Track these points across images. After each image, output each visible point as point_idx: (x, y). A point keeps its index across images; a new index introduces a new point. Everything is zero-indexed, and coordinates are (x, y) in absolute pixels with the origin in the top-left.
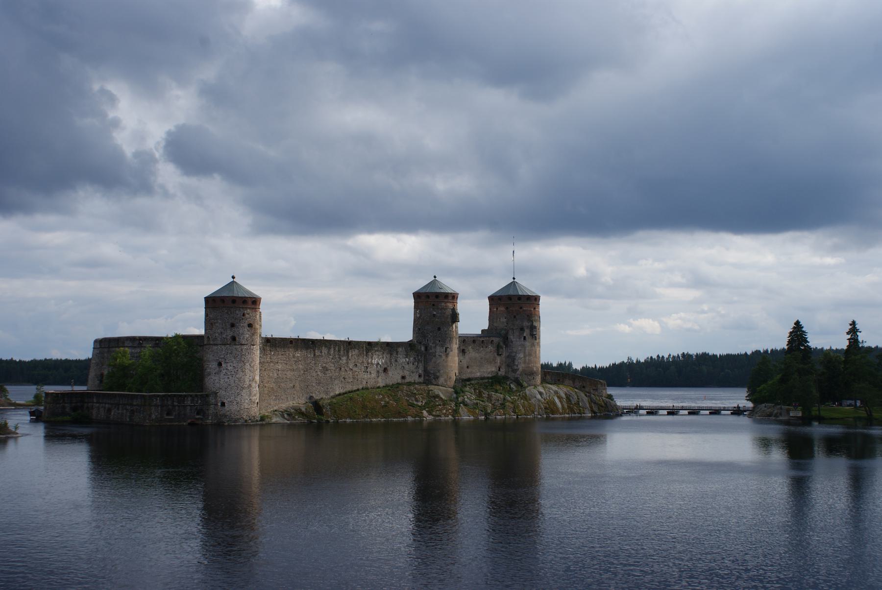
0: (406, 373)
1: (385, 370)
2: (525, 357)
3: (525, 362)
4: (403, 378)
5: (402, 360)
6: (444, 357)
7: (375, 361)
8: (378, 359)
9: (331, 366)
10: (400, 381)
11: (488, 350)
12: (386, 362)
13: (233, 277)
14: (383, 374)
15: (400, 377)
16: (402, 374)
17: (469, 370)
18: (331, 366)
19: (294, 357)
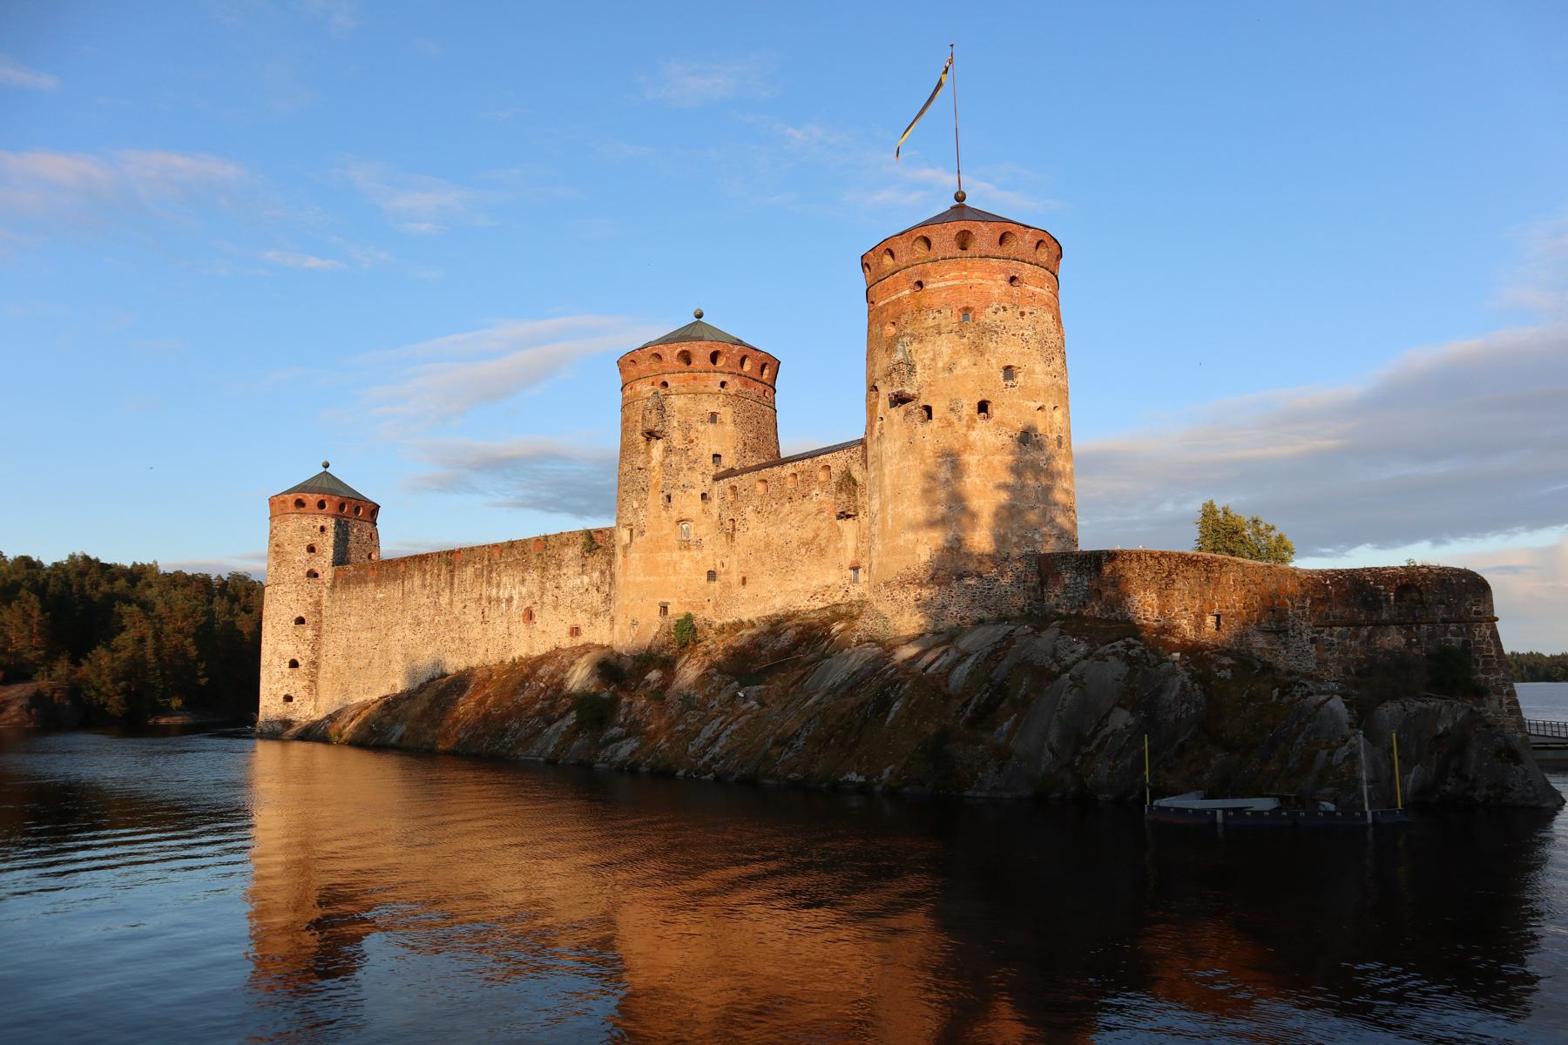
0: (581, 619)
1: (529, 615)
2: (883, 508)
3: (883, 531)
4: (575, 631)
5: (574, 579)
7: (504, 594)
8: (513, 587)
9: (425, 615)
10: (566, 642)
11: (809, 506)
12: (531, 595)
14: (521, 627)
15: (566, 630)
16: (571, 622)
17: (745, 593)
18: (425, 615)
19: (374, 600)
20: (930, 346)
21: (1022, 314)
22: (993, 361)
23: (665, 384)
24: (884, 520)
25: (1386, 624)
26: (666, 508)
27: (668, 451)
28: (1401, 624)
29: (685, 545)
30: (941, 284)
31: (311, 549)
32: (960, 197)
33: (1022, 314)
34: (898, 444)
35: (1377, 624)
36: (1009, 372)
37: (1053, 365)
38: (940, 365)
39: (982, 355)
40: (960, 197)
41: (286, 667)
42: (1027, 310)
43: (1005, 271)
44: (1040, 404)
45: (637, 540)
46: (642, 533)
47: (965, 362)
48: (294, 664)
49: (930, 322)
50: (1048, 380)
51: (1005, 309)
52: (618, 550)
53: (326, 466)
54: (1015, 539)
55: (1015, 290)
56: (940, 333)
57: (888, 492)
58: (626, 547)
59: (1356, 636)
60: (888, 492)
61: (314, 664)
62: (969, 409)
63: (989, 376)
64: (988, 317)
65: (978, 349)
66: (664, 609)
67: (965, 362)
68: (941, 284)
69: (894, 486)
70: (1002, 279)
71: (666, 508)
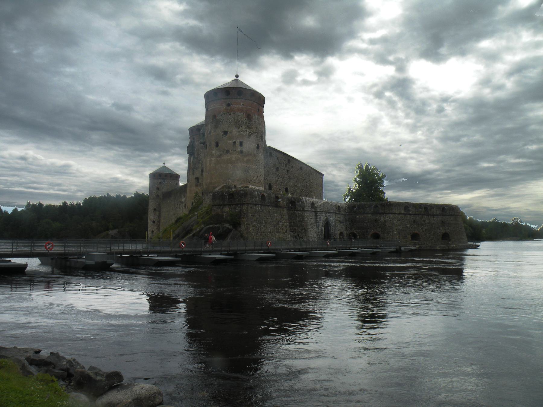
13: (164, 164)
14: (184, 209)
21: (230, 114)
23: (194, 139)
25: (226, 205)
26: (193, 174)
27: (194, 158)
28: (229, 205)
29: (197, 185)
31: (158, 189)
33: (230, 114)
35: (225, 205)
36: (225, 133)
37: (241, 128)
41: (152, 223)
42: (232, 113)
47: (213, 131)
48: (154, 222)
50: (238, 133)
53: (164, 164)
55: (228, 108)
59: (220, 208)
61: (159, 222)
62: (213, 144)
65: (216, 127)
66: (192, 204)
67: (213, 131)
71: (193, 174)
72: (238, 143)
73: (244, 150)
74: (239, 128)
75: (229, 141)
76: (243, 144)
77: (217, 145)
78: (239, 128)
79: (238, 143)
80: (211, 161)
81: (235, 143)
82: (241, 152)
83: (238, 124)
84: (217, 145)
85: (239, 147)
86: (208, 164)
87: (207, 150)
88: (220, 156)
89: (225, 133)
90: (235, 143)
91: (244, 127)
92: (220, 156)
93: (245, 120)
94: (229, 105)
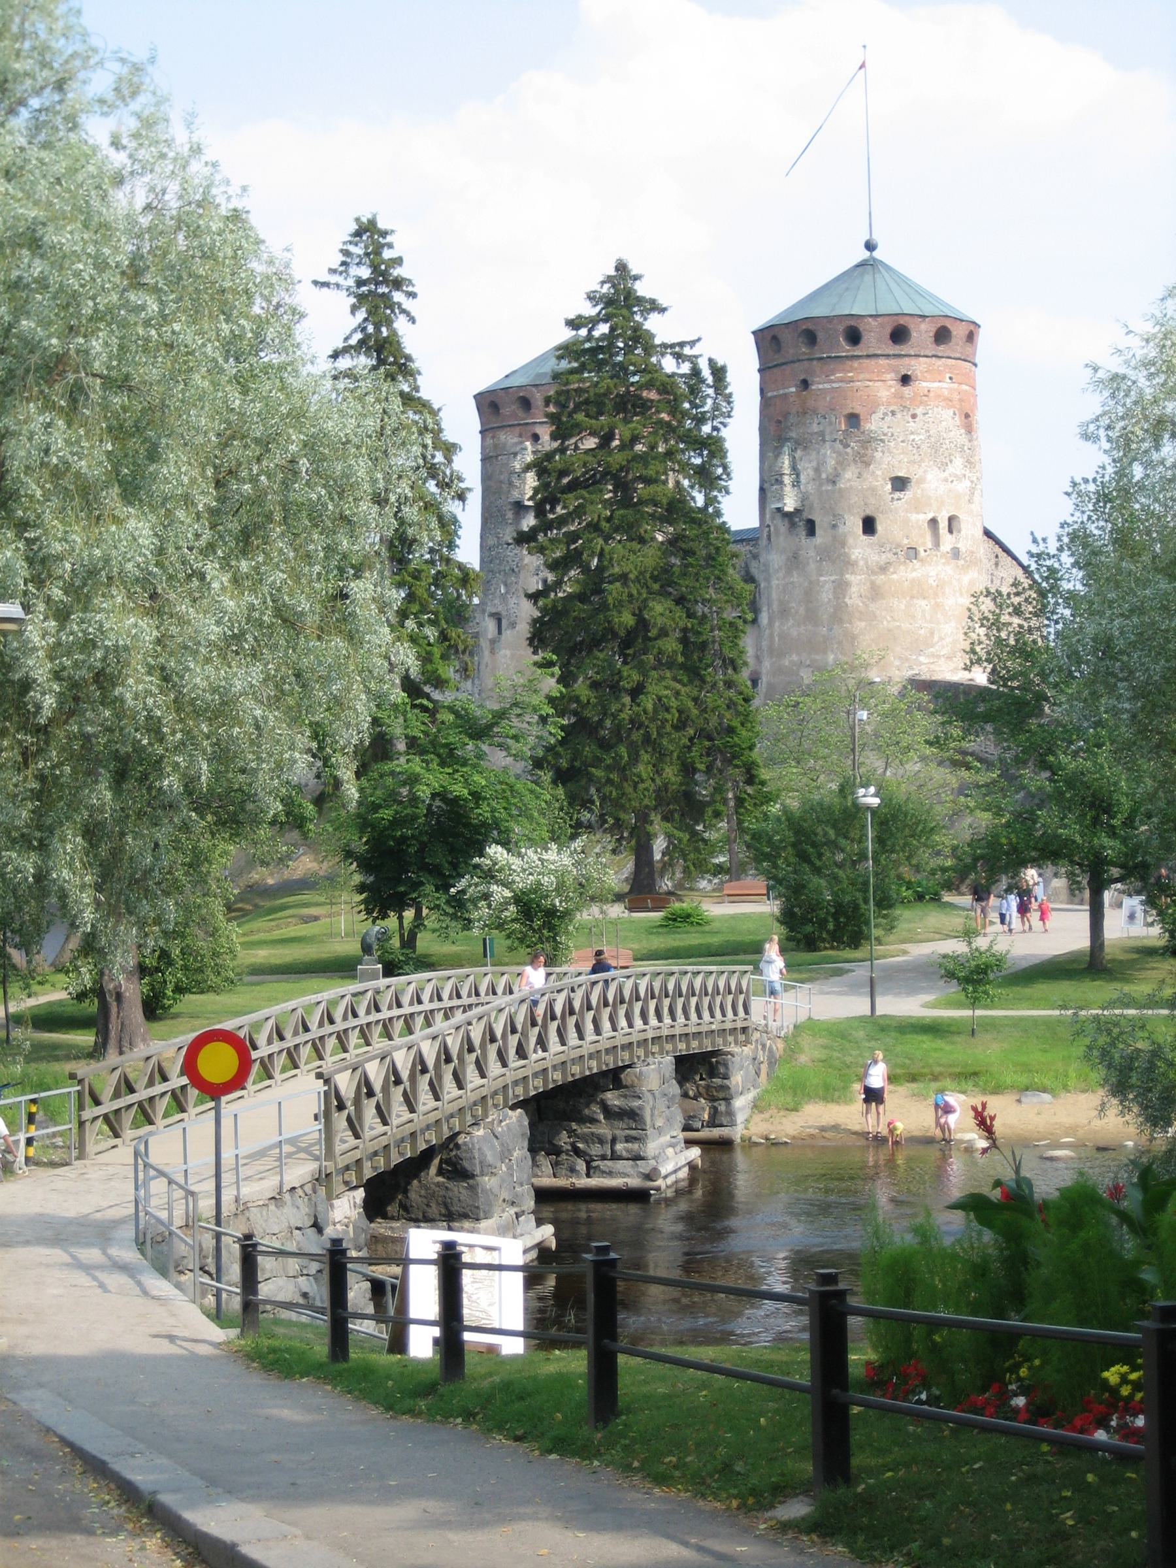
6: (486, 653)
20: (813, 455)
21: (914, 416)
22: (879, 473)
24: (771, 635)
30: (827, 386)
32: (870, 246)
33: (914, 416)
34: (784, 557)
36: (900, 484)
37: (951, 469)
38: (824, 476)
39: (867, 464)
40: (870, 246)
42: (919, 411)
43: (894, 369)
44: (930, 516)
45: (507, 634)
46: (513, 625)
49: (815, 428)
51: (893, 413)
52: (484, 644)
54: (897, 663)
55: (907, 391)
56: (824, 441)
57: (775, 607)
58: (493, 642)
60: (775, 607)
63: (873, 489)
64: (873, 424)
65: (864, 460)
68: (827, 386)
69: (781, 603)
70: (891, 378)
72: (943, 525)
73: (963, 549)
74: (943, 466)
75: (914, 517)
76: (954, 524)
77: (869, 525)
78: (943, 466)
79: (943, 525)
80: (841, 587)
81: (933, 522)
82: (956, 553)
83: (939, 454)
84: (869, 525)
85: (949, 536)
86: (826, 595)
87: (820, 538)
88: (883, 569)
89: (900, 484)
90: (933, 522)
91: (958, 462)
92: (883, 569)
93: (958, 435)
94: (905, 380)
